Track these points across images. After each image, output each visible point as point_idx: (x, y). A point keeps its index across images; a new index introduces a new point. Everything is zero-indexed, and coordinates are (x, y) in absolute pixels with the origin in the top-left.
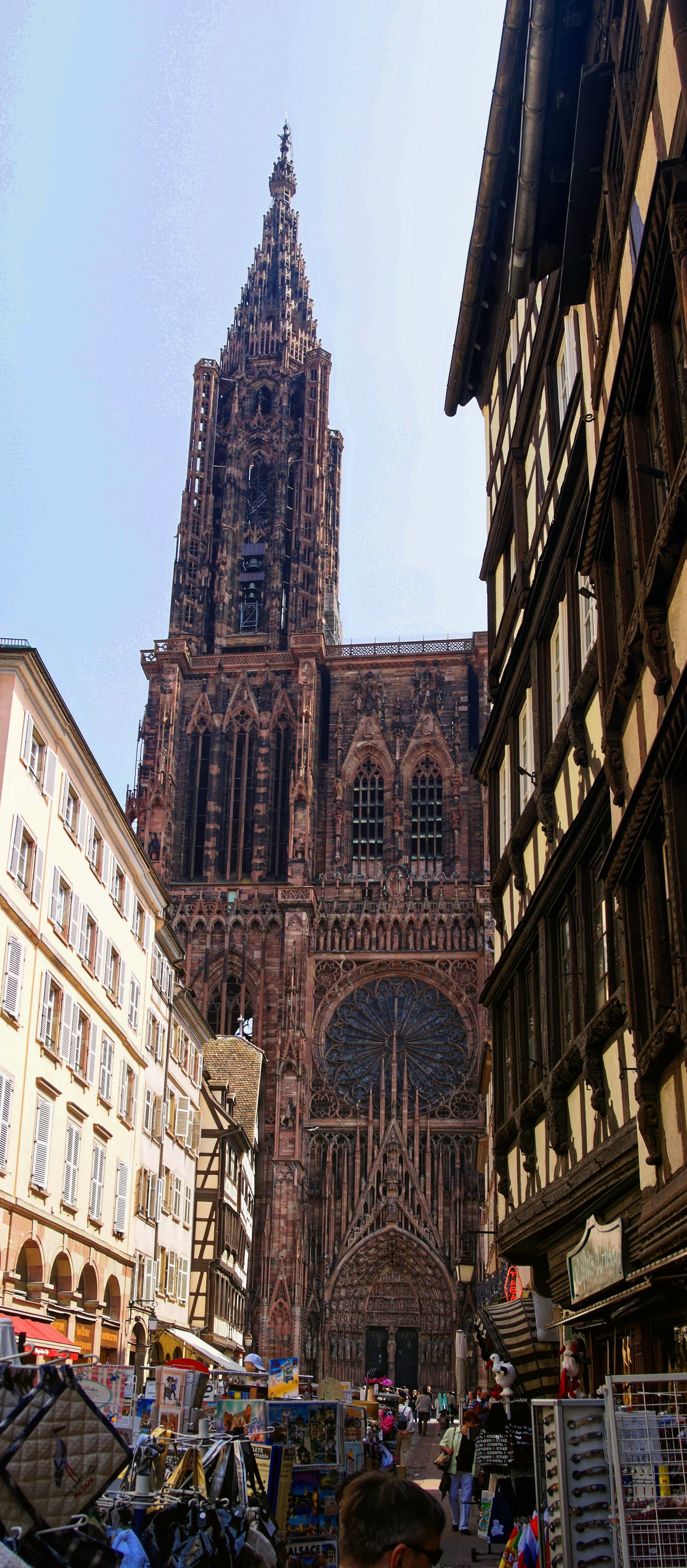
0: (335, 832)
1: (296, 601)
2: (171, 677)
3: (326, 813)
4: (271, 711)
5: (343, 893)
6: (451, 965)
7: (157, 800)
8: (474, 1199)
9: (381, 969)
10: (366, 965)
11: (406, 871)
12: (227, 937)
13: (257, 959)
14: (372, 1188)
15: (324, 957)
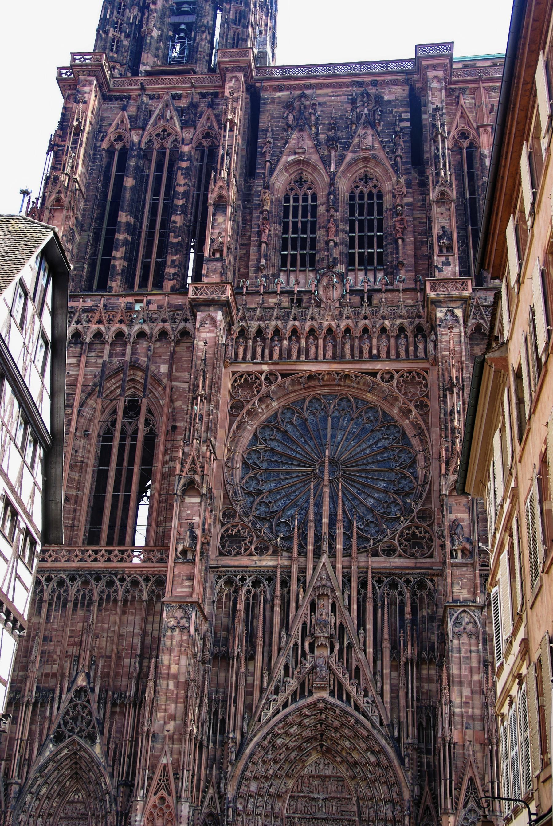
0: (260, 240)
1: (227, 35)
2: (87, 89)
3: (251, 226)
4: (195, 128)
5: (268, 302)
6: (396, 376)
7: (58, 200)
8: (431, 662)
9: (312, 383)
10: (292, 377)
11: (342, 278)
12: (129, 348)
13: (163, 373)
14: (296, 644)
15: (243, 368)
